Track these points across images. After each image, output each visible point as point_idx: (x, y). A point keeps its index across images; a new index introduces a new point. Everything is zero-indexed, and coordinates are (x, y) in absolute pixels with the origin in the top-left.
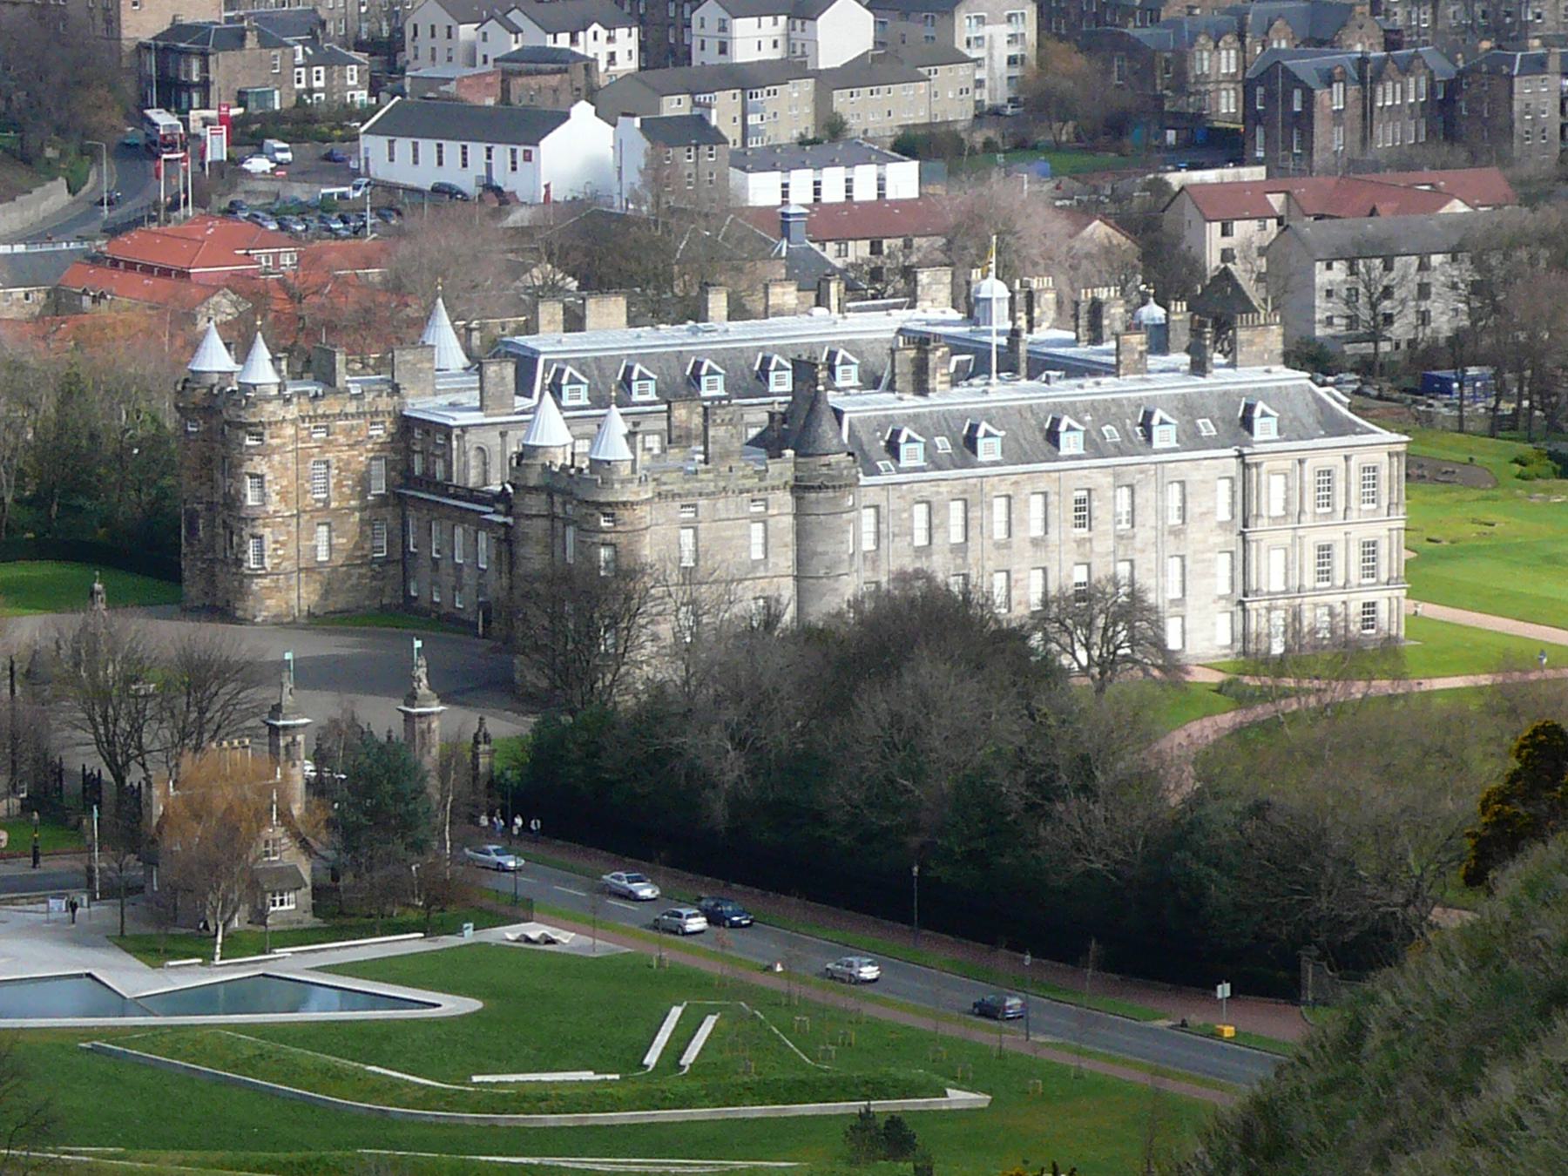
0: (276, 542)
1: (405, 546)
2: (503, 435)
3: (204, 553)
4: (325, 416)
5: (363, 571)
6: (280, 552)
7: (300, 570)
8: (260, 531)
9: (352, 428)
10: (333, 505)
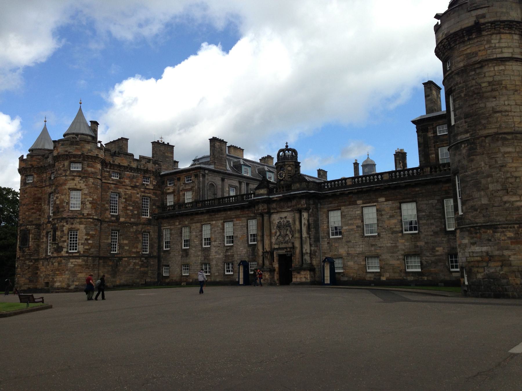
0: (87, 234)
1: (160, 247)
2: (223, 180)
3: (30, 255)
4: (119, 166)
5: (137, 261)
6: (90, 242)
7: (100, 258)
8: (77, 226)
9: (134, 177)
10: (122, 220)
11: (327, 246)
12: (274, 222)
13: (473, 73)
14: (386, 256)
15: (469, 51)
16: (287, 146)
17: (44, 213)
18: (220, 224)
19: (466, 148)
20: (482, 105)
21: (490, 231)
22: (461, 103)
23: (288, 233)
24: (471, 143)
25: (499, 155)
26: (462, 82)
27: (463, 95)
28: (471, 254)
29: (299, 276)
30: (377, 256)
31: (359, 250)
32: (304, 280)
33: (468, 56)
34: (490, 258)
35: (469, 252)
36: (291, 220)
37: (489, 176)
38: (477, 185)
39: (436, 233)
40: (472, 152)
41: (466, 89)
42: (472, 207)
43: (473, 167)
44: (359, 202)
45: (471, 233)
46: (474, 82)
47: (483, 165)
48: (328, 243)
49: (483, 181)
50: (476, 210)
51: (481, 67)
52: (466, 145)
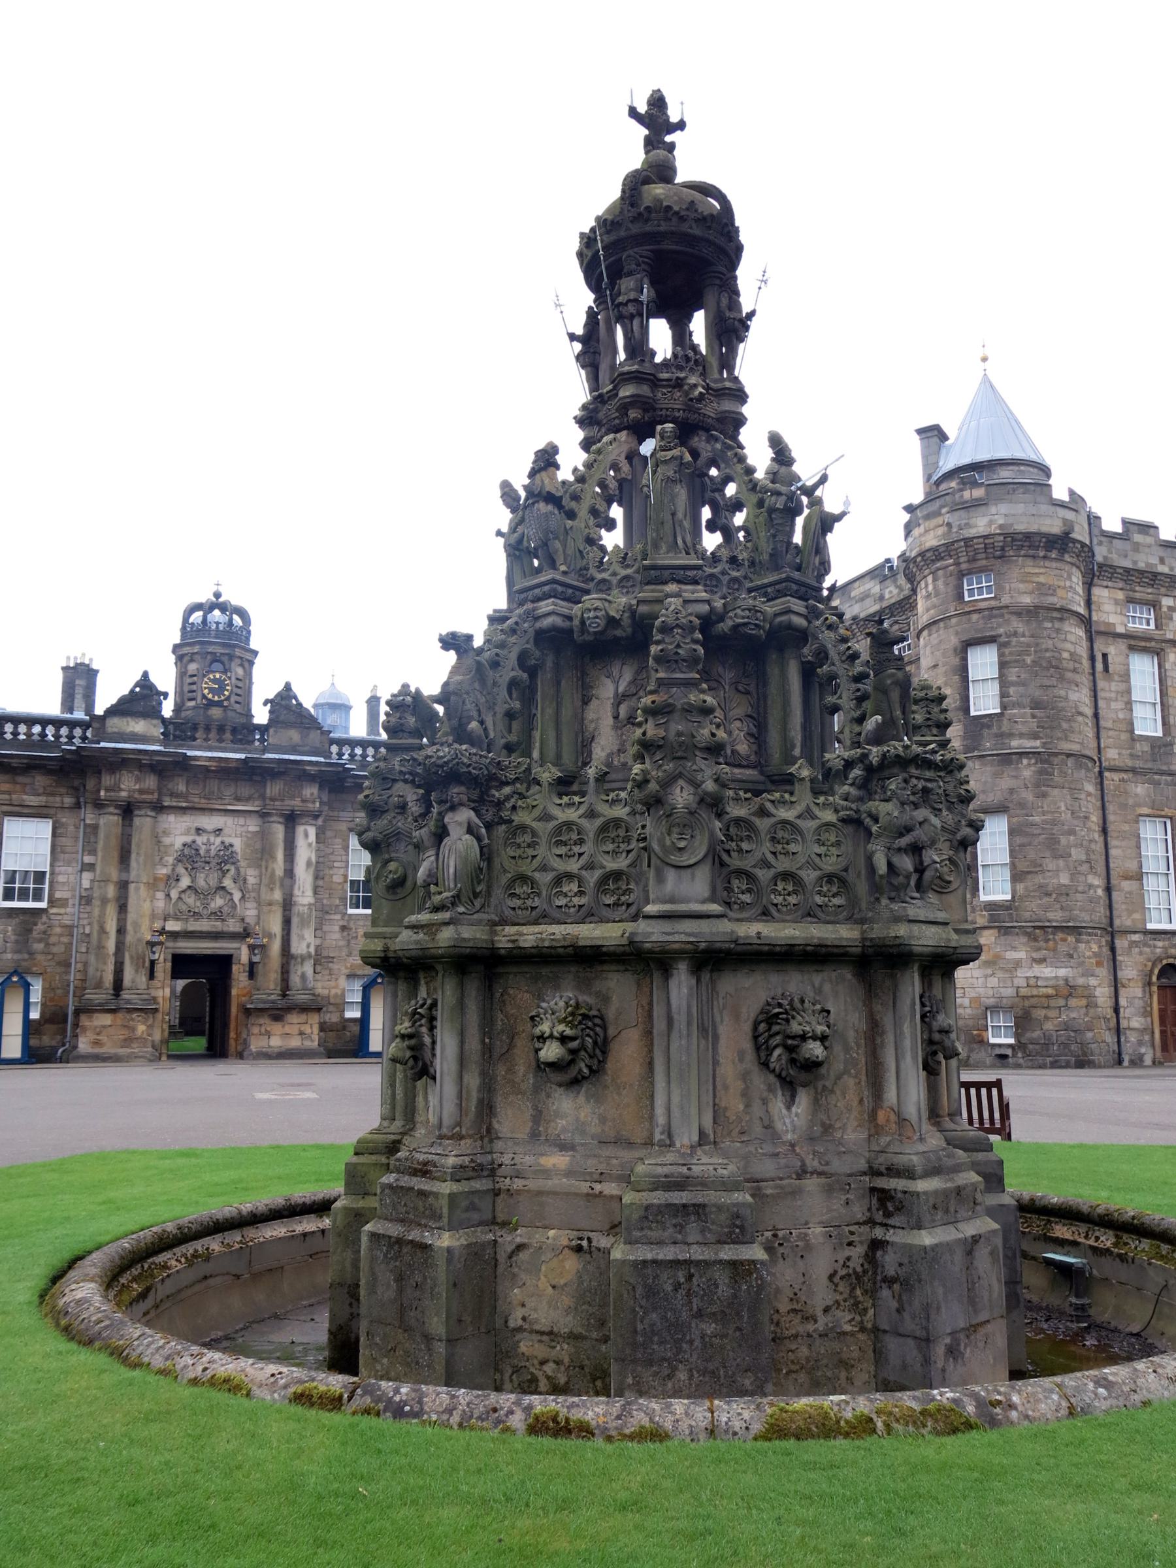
11: (337, 936)
12: (167, 840)
13: (1049, 625)
15: (1042, 579)
16: (217, 595)
19: (1033, 768)
20: (1062, 693)
21: (1071, 939)
22: (1023, 676)
23: (228, 882)
24: (1045, 759)
25: (1083, 796)
26: (1027, 634)
27: (1029, 660)
28: (1032, 982)
29: (276, 1028)
32: (295, 1043)
34: (1069, 990)
35: (1027, 978)
36: (238, 844)
37: (1072, 832)
41: (1036, 652)
42: (1041, 887)
43: (1046, 809)
45: (1035, 940)
46: (1050, 642)
47: (1063, 808)
48: (343, 928)
49: (1063, 840)
50: (1048, 895)
51: (1061, 619)
52: (1033, 761)
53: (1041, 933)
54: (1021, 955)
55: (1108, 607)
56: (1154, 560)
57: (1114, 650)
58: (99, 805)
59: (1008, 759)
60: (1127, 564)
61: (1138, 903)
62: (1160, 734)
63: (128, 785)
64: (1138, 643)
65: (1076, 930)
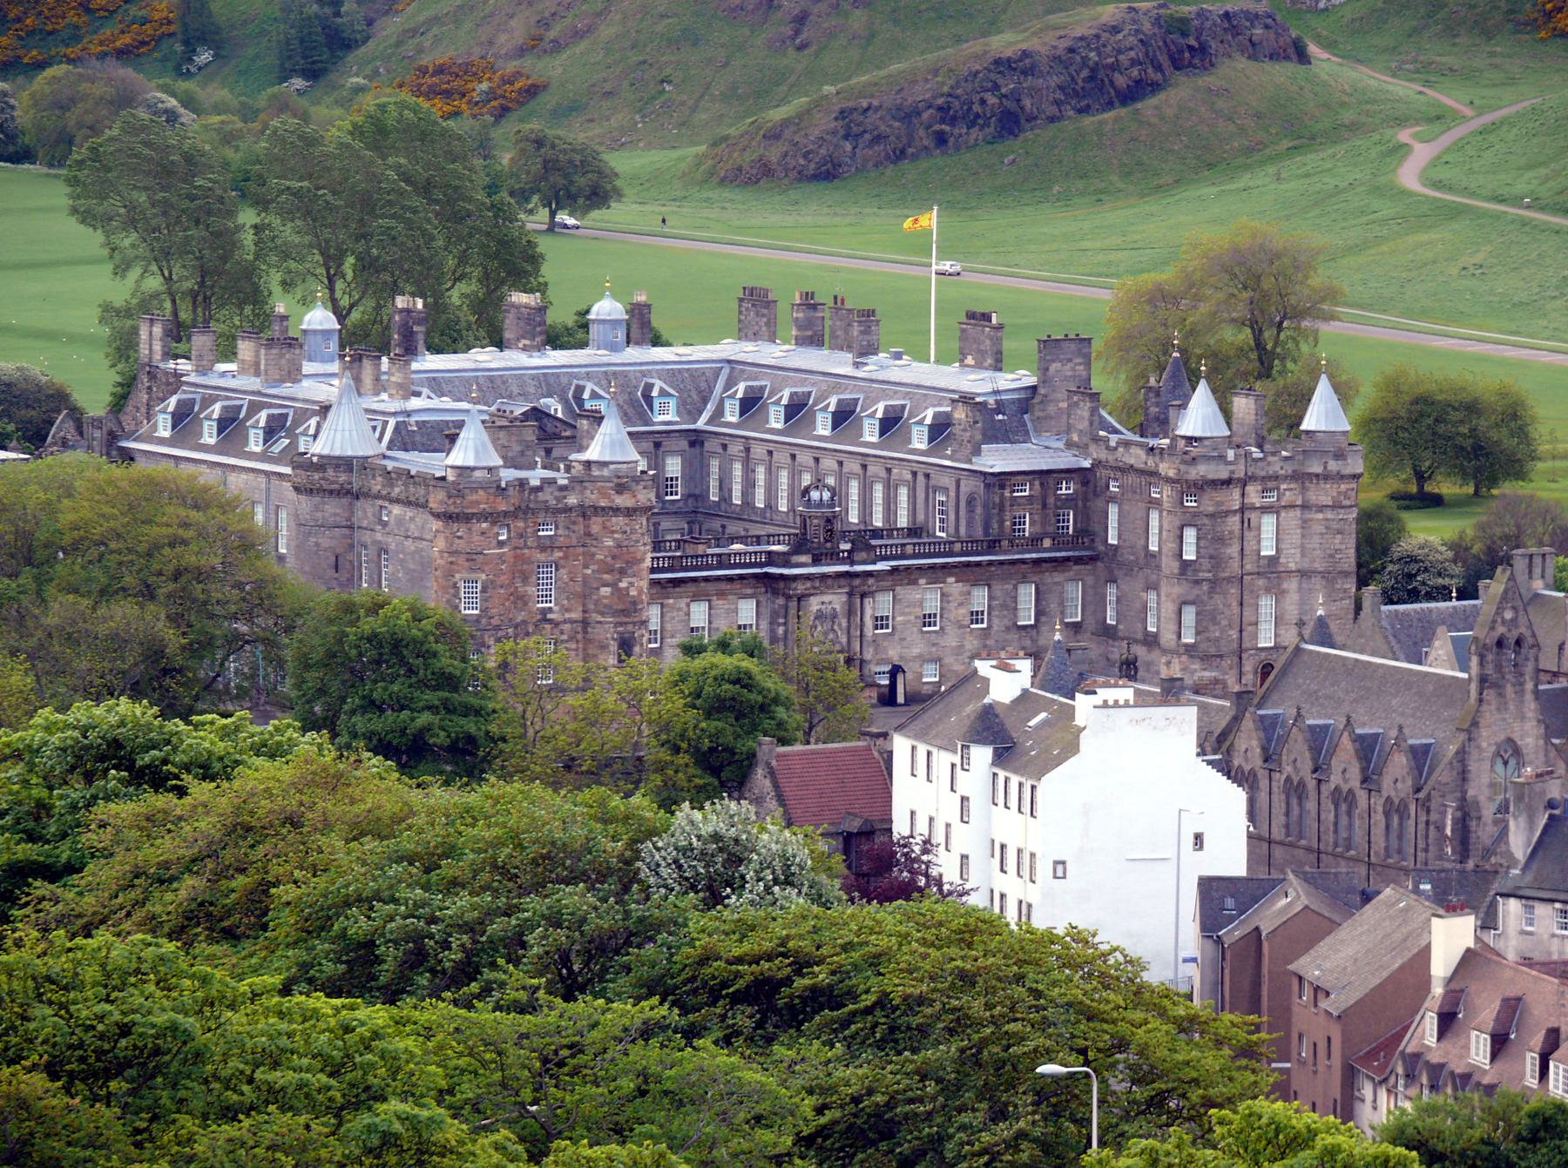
14: (947, 661)
17: (526, 604)
18: (683, 605)
30: (938, 660)
31: (916, 651)
33: (1219, 504)
36: (838, 607)
38: (1214, 621)
39: (1008, 629)
40: (1212, 591)
44: (922, 581)
53: (1206, 659)
54: (1196, 666)
55: (1253, 494)
56: (1277, 468)
57: (1253, 516)
58: (788, 597)
59: (1197, 582)
60: (1263, 473)
61: (1255, 637)
62: (1273, 553)
63: (800, 588)
64: (1266, 509)
65: (1221, 656)
